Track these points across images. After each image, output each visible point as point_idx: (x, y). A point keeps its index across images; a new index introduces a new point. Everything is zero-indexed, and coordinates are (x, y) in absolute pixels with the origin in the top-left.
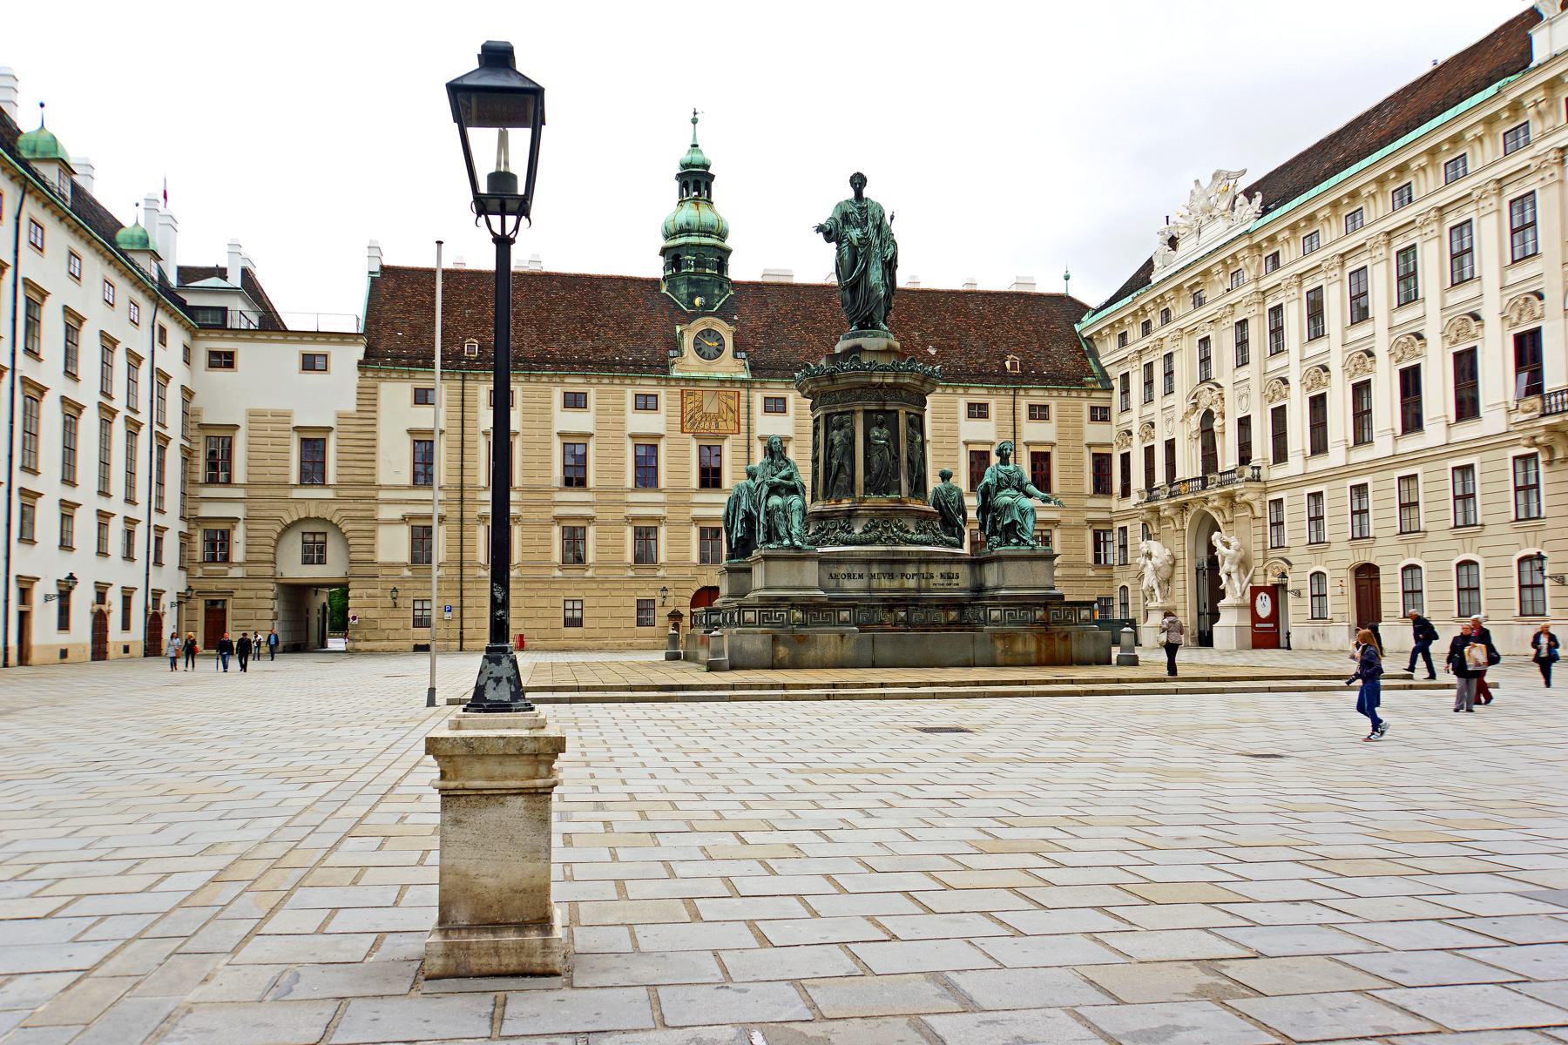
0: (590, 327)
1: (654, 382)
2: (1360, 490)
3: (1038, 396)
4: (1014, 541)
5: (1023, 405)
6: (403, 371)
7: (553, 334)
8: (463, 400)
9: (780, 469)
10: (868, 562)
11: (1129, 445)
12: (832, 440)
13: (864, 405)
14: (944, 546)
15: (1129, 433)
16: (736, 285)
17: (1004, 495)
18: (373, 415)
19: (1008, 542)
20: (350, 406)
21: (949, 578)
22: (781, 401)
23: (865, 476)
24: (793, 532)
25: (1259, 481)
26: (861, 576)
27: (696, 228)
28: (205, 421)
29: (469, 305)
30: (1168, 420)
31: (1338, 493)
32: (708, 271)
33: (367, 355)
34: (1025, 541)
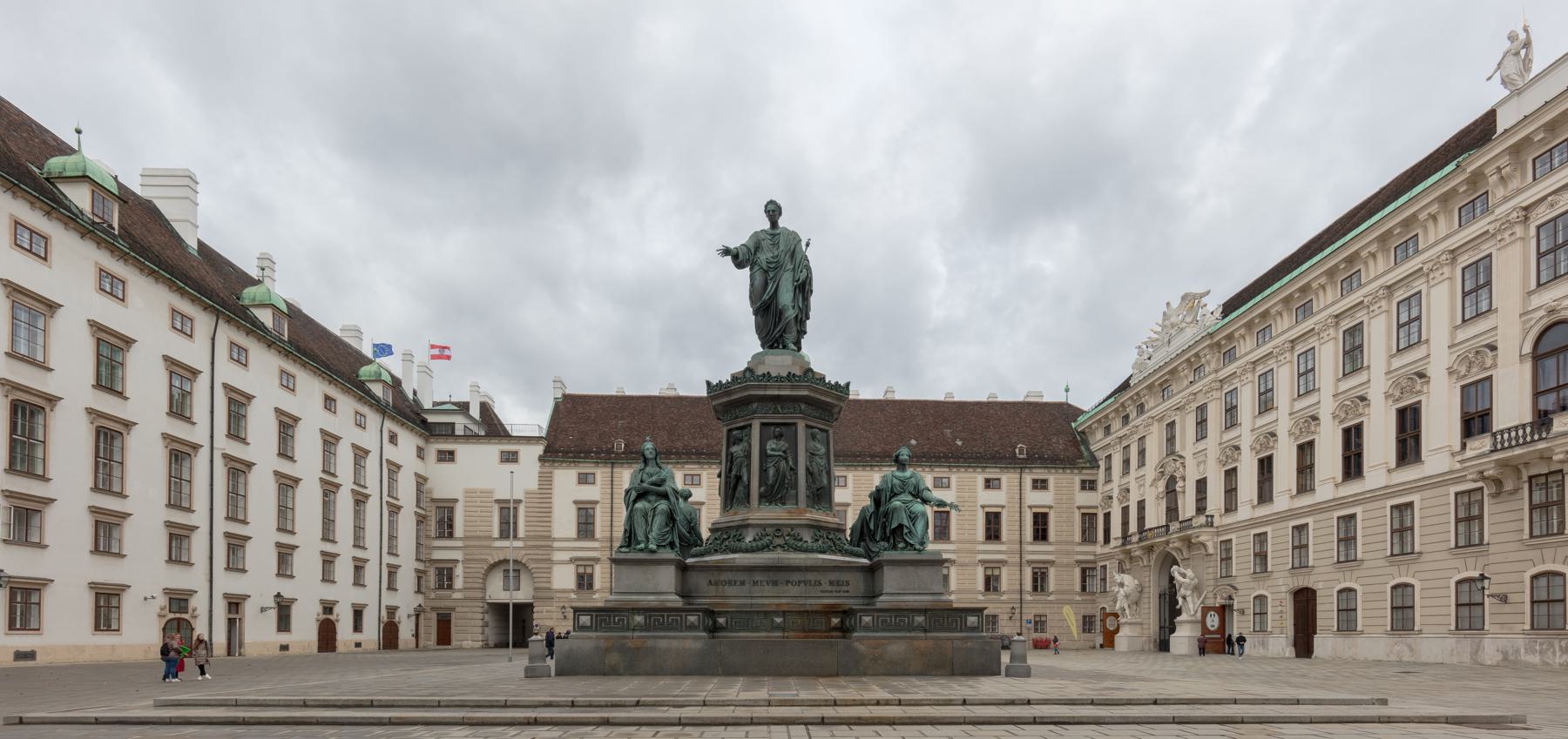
2: (1301, 529)
3: (1040, 474)
5: (1028, 479)
6: (570, 462)
7: (679, 435)
8: (612, 481)
10: (750, 569)
11: (1110, 506)
12: (732, 454)
13: (760, 418)
14: (843, 555)
15: (1111, 498)
18: (549, 491)
19: (894, 547)
20: (533, 484)
21: (838, 585)
22: (843, 479)
23: (760, 486)
25: (1212, 526)
26: (743, 583)
28: (436, 496)
29: (622, 418)
30: (1141, 486)
31: (1282, 532)
33: (545, 452)
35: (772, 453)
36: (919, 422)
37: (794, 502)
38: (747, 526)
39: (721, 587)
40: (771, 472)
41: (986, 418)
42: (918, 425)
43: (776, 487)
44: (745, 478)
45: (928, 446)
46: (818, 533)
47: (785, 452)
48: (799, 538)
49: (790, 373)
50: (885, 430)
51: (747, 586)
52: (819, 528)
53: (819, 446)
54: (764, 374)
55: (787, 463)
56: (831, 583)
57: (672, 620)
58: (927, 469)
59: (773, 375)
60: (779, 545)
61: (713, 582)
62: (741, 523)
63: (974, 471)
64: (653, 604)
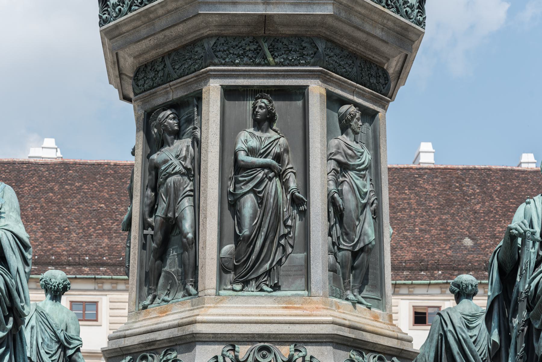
35: (251, 159)
37: (301, 282)
47: (278, 158)
50: (418, 220)
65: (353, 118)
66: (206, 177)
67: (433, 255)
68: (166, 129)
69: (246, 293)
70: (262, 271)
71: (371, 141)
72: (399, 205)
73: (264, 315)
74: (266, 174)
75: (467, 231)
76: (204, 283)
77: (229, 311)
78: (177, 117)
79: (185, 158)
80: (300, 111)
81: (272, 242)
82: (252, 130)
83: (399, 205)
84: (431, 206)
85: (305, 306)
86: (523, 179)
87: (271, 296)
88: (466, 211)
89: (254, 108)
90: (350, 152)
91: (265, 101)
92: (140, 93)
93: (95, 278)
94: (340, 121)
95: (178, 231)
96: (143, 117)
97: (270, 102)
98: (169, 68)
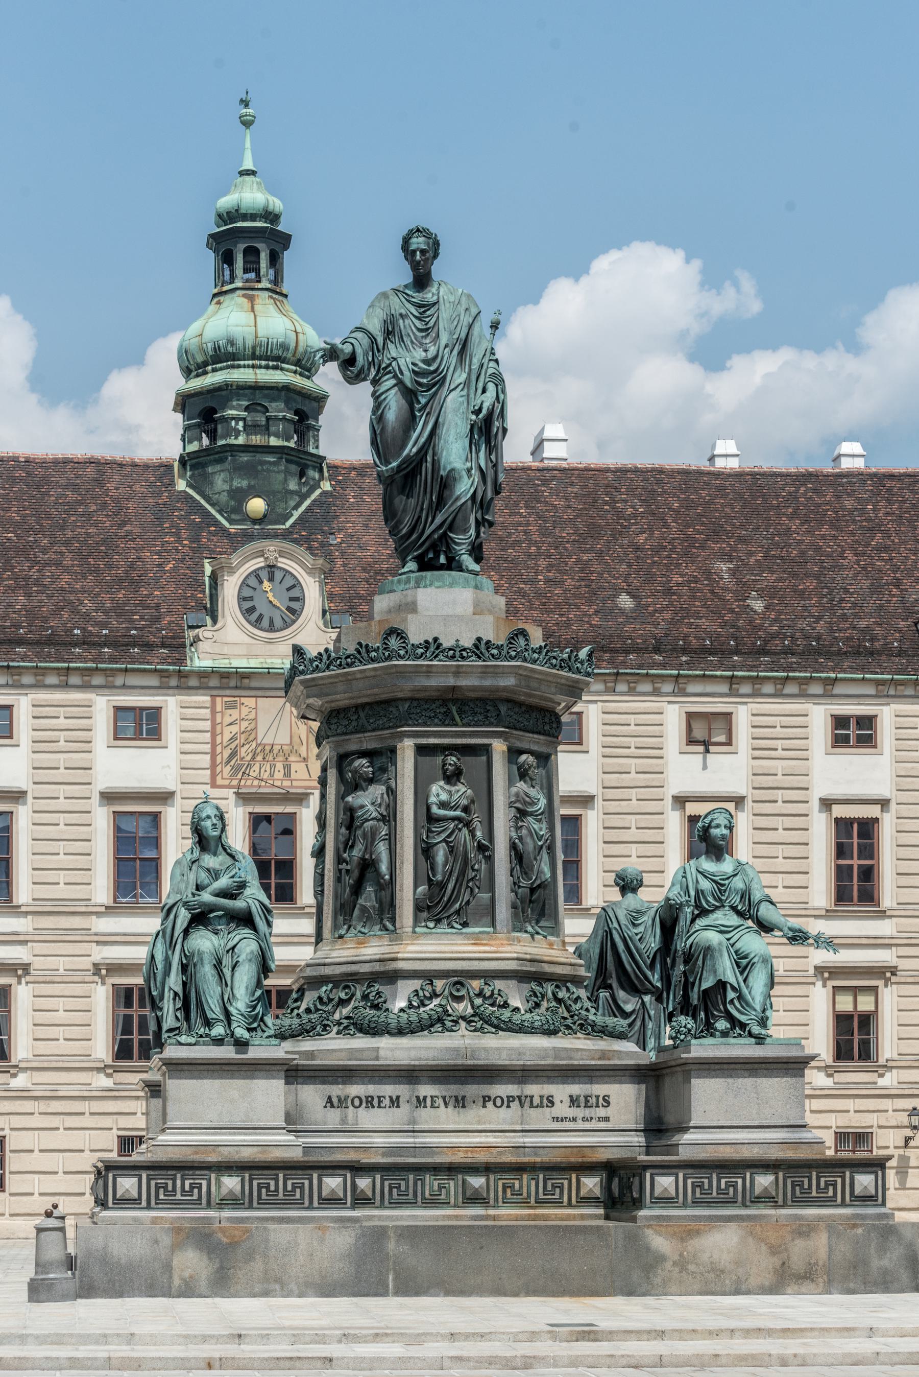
0: (22, 567)
1: (154, 681)
4: (722, 1025)
9: (215, 875)
16: (333, 468)
17: (706, 928)
23: (416, 887)
24: (232, 1009)
26: (395, 1102)
27: (249, 352)
32: (274, 441)
34: (743, 1026)
35: (442, 812)
36: (641, 539)
37: (488, 919)
38: (392, 977)
39: (351, 1108)
40: (441, 854)
41: (832, 526)
42: (638, 548)
43: (450, 886)
44: (384, 868)
45: (668, 615)
46: (538, 989)
47: (466, 809)
48: (500, 1001)
49: (479, 639)
50: (543, 563)
51: (405, 1108)
52: (540, 978)
53: (533, 792)
54: (427, 642)
55: (472, 833)
56: (574, 1101)
57: (294, 1187)
58: (668, 687)
59: (447, 643)
60: (463, 1018)
61: (335, 1100)
62: (378, 967)
63: (803, 695)
64: (247, 1154)
65: (530, 767)
66: (402, 827)
67: (568, 624)
68: (361, 776)
69: (439, 931)
70: (452, 910)
71: (544, 781)
72: (510, 534)
73: (457, 952)
74: (456, 826)
75: (624, 581)
76: (402, 922)
77: (425, 948)
78: (372, 764)
79: (380, 805)
80: (485, 764)
81: (461, 885)
82: (442, 783)
83: (510, 534)
84: (564, 538)
85: (491, 942)
86: (719, 488)
87: (462, 933)
88: (621, 546)
89: (444, 765)
90: (527, 799)
91: (454, 758)
92: (332, 736)
93: (8, 667)
94: (519, 769)
95: (373, 869)
96: (335, 758)
97: (459, 759)
98: (363, 720)
